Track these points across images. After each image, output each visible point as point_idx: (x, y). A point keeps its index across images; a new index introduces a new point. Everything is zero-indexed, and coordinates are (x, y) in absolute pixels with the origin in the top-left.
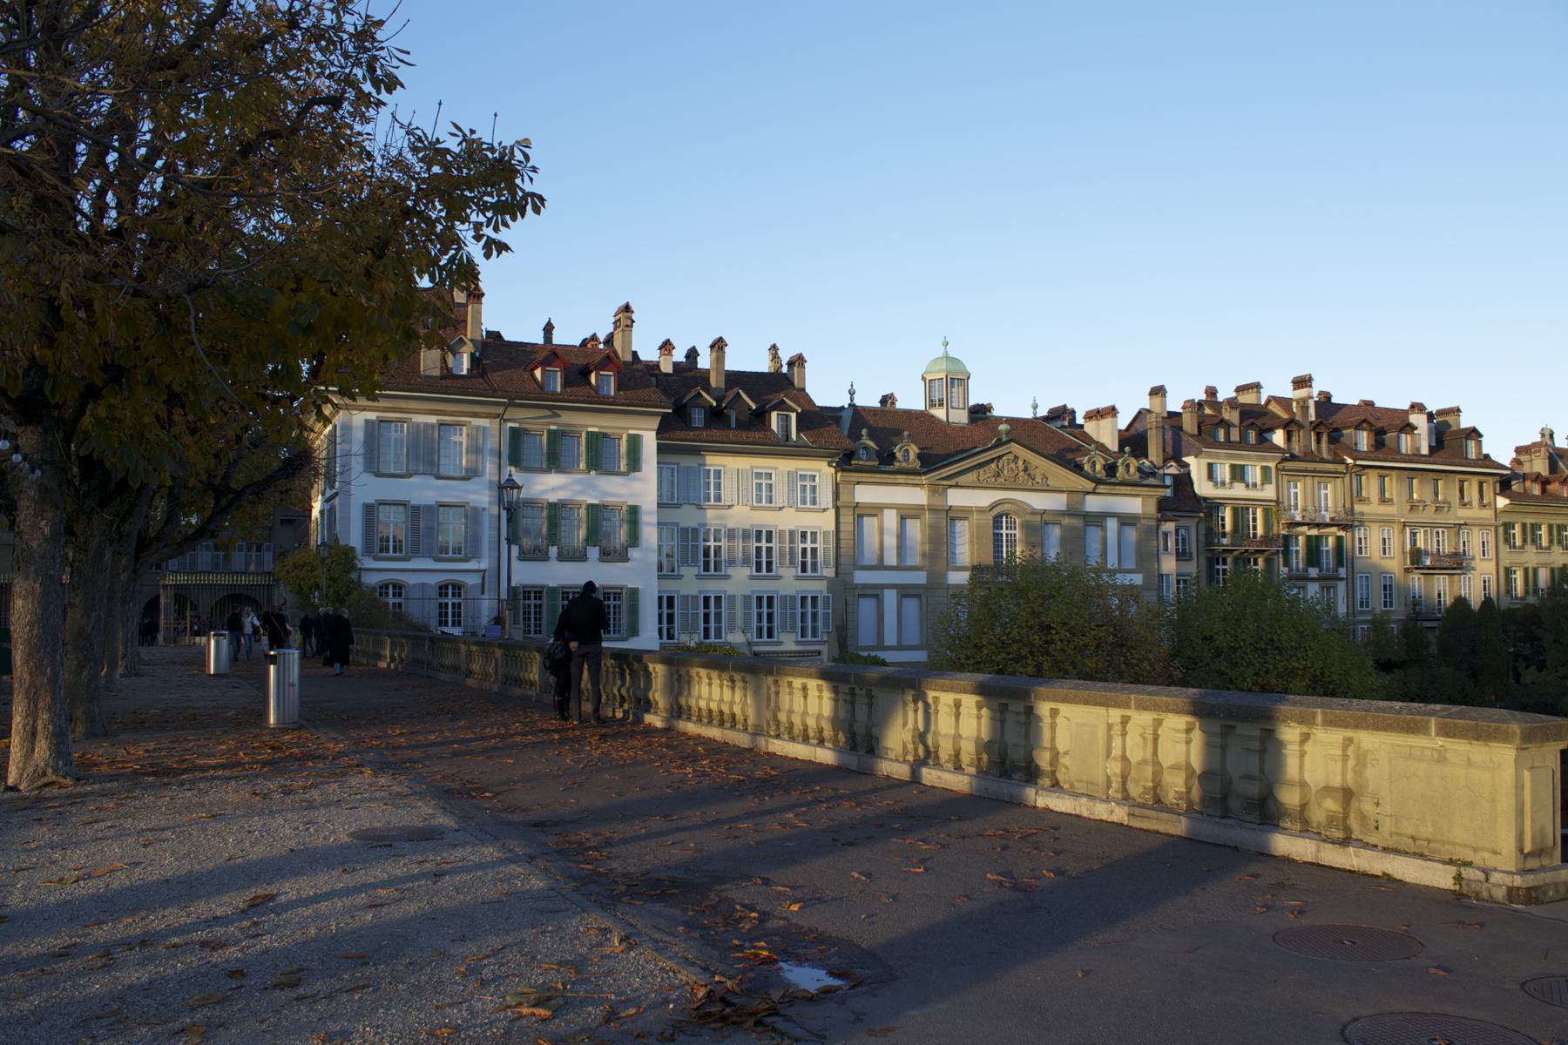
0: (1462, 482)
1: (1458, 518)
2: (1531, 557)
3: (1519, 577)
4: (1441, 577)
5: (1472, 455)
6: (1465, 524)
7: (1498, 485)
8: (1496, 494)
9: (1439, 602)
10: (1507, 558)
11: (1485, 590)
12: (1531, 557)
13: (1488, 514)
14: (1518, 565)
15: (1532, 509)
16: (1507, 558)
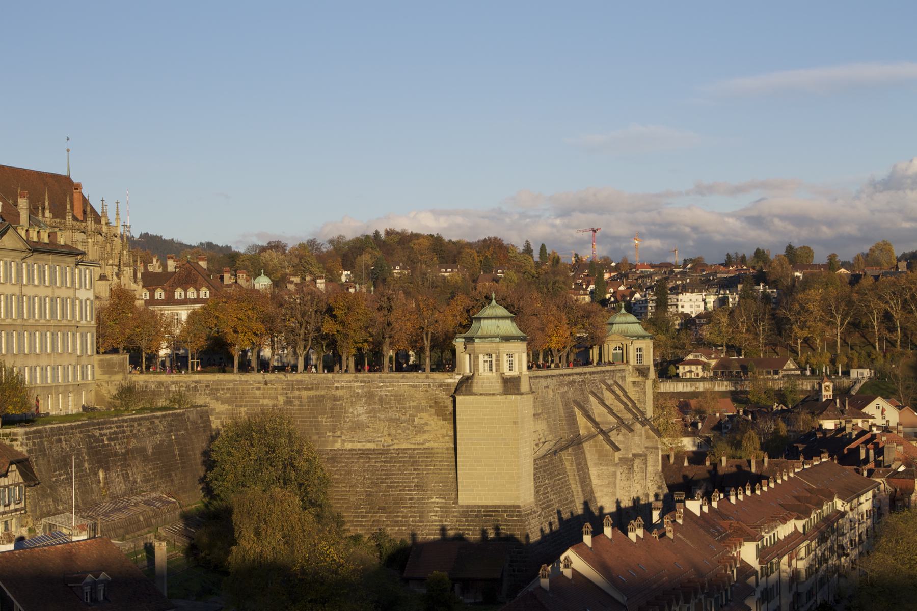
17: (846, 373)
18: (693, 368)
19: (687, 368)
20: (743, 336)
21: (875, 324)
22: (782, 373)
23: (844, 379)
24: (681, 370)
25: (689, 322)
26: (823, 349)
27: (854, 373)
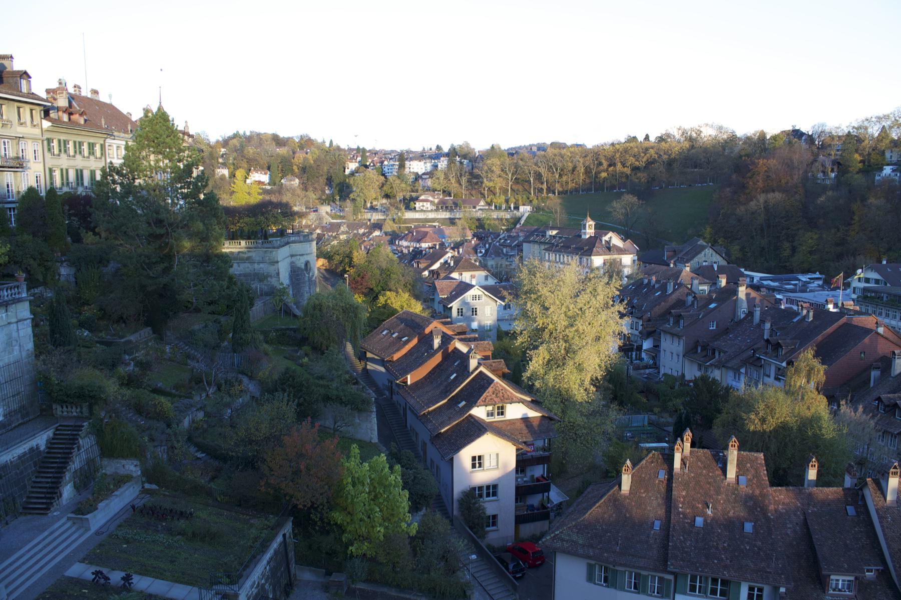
0: (19, 108)
1: (18, 133)
2: (64, 162)
3: (57, 175)
4: (9, 173)
5: (24, 90)
6: (23, 138)
7: (42, 112)
8: (42, 118)
9: (8, 190)
10: (51, 162)
11: (37, 183)
12: (64, 162)
13: (37, 131)
14: (57, 166)
15: (65, 130)
16: (51, 162)
17: (517, 208)
18: (425, 204)
19: (421, 204)
20: (454, 186)
21: (532, 179)
22: (478, 208)
23: (515, 212)
24: (418, 205)
25: (418, 177)
26: (500, 194)
27: (522, 208)
